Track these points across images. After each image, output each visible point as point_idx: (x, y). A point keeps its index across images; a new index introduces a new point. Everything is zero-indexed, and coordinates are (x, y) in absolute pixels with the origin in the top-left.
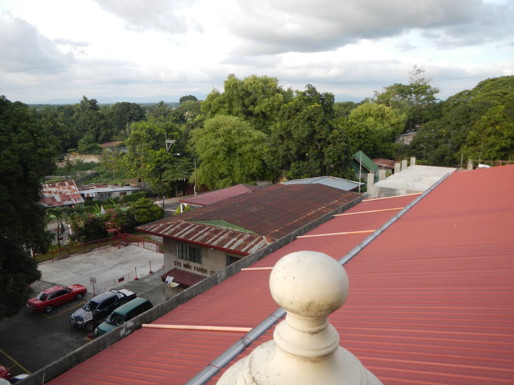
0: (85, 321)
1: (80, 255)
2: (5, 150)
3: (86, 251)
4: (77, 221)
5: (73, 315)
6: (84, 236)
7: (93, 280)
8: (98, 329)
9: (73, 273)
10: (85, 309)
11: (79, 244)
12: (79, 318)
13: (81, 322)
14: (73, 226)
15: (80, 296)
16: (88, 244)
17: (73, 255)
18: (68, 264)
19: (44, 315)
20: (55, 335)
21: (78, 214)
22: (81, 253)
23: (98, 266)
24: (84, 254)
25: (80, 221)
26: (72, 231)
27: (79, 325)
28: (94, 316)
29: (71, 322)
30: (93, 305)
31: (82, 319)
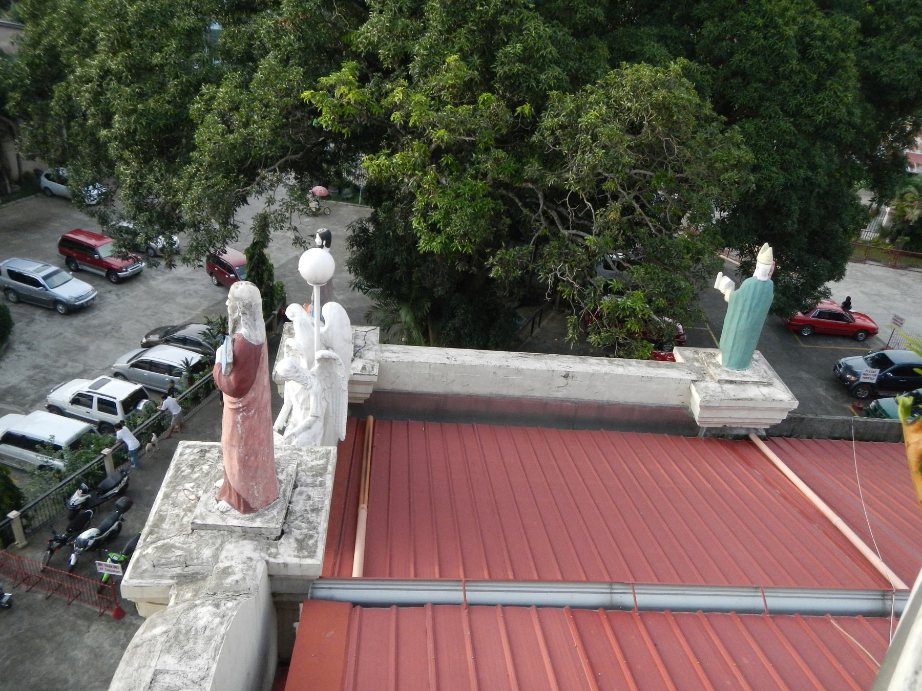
0: (862, 380)
1: (884, 268)
2: (907, 45)
3: (898, 264)
4: (908, 206)
5: (843, 360)
6: (907, 238)
7: (898, 321)
8: (877, 403)
9: (862, 292)
10: (866, 359)
11: (890, 248)
12: (849, 369)
13: (853, 378)
14: (894, 212)
15: (861, 336)
16: (907, 255)
17: (872, 263)
18: (859, 274)
19: (797, 338)
20: (804, 375)
21: (917, 194)
22: (886, 265)
23: (909, 300)
24: (892, 269)
25: (912, 208)
26: (889, 221)
27: (847, 380)
28: (880, 380)
29: (835, 368)
30: (881, 362)
31: (855, 374)
